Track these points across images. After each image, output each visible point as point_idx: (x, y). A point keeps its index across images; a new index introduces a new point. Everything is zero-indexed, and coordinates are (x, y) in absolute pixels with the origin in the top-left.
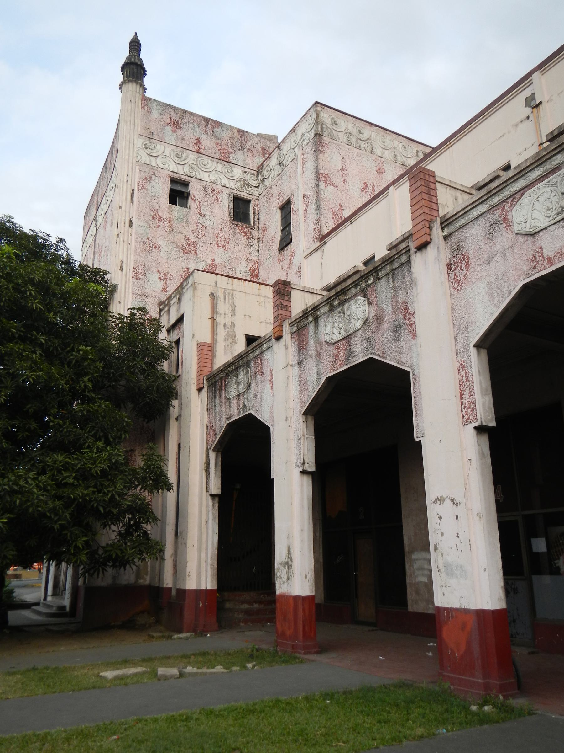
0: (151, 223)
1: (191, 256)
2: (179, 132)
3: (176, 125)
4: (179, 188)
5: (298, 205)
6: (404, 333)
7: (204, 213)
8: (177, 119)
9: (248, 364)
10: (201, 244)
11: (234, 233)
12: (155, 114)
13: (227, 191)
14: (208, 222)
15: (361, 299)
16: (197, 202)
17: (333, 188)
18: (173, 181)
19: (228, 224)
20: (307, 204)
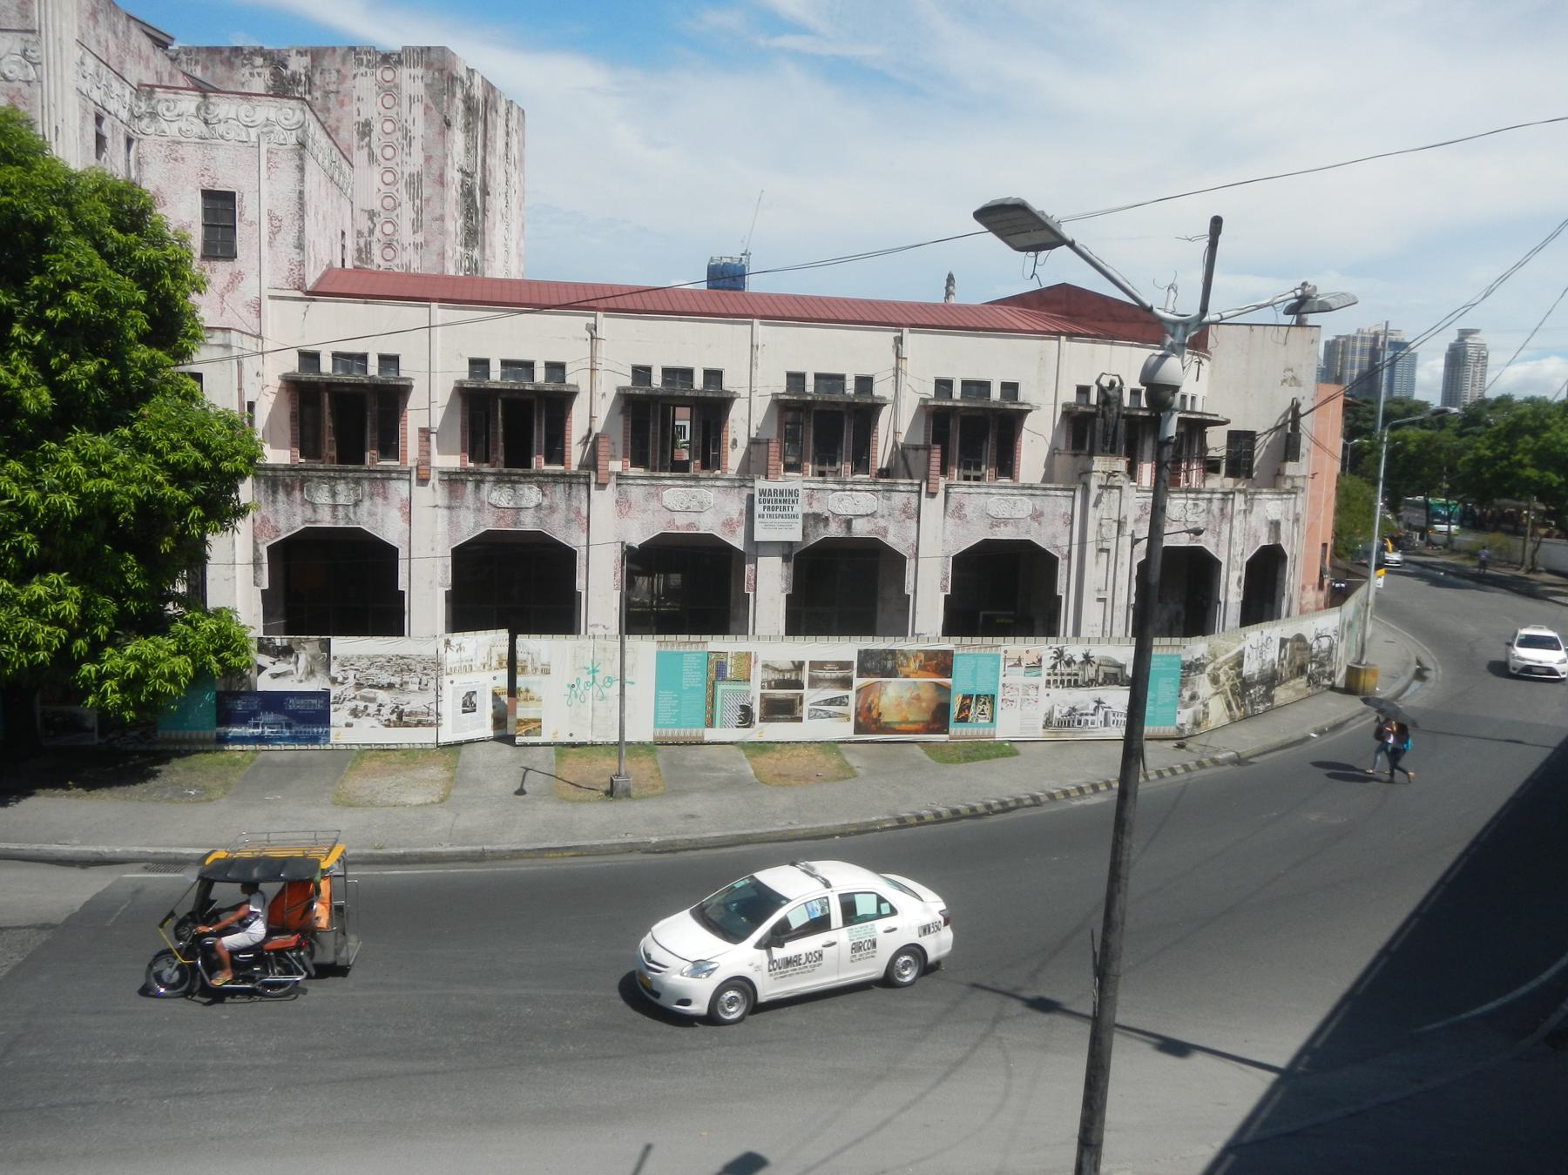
5: (248, 211)
6: (574, 526)
9: (358, 481)
15: (536, 489)
20: (275, 231)
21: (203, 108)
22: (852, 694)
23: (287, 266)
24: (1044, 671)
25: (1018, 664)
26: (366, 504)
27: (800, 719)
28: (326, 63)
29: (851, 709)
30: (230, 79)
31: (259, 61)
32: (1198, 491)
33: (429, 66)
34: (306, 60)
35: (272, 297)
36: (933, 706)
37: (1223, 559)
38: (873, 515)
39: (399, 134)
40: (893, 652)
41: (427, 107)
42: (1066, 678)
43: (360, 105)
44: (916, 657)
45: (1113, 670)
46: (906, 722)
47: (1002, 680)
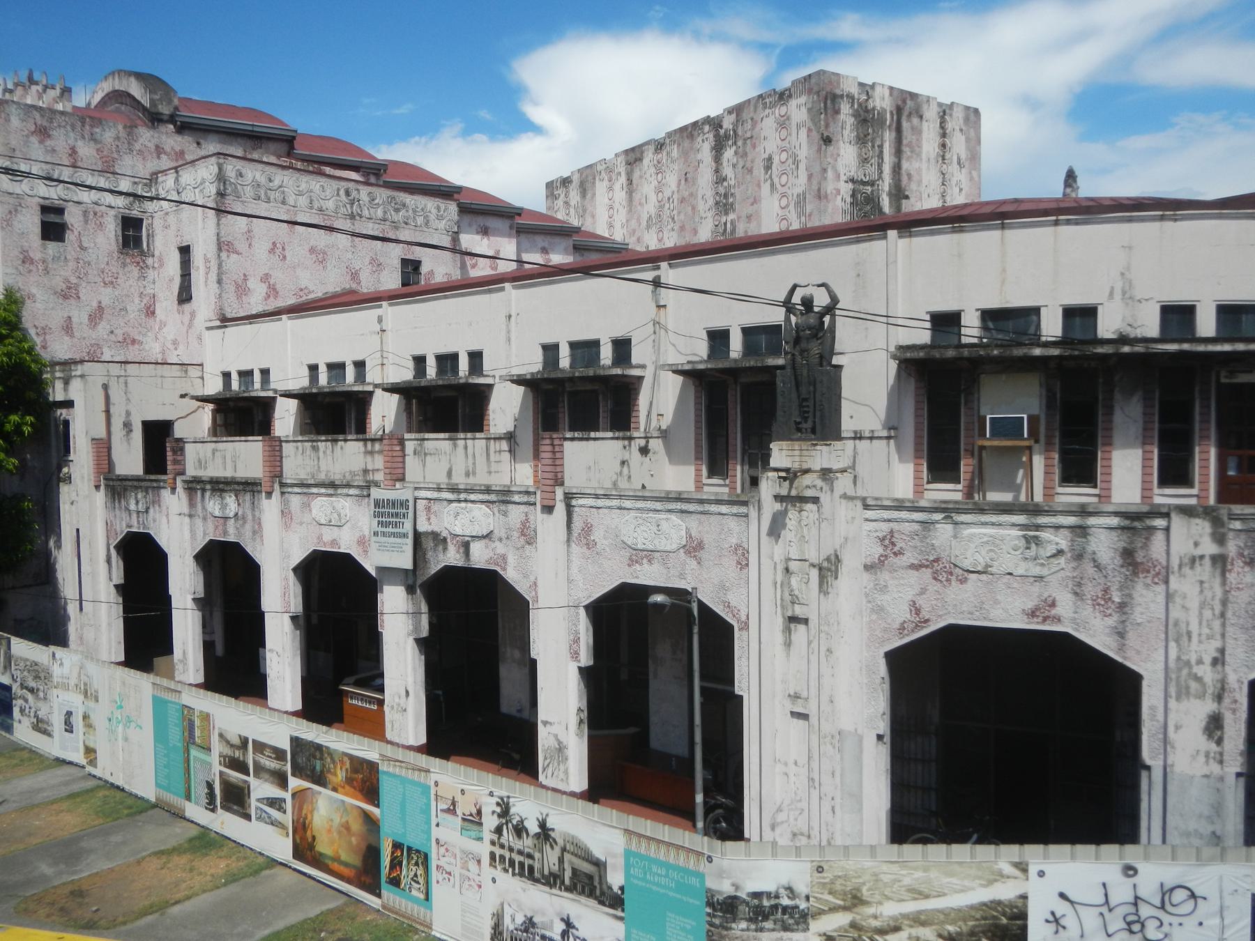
0: (21, 268)
1: (72, 301)
2: (48, 143)
3: (43, 133)
4: (52, 218)
7: (85, 245)
8: (45, 124)
10: (84, 284)
11: (124, 265)
12: (15, 122)
13: (112, 212)
14: (91, 256)
16: (76, 233)
17: (235, 256)
18: (45, 209)
19: (116, 255)
21: (177, 180)
22: (288, 796)
23: (213, 300)
24: (488, 835)
25: (452, 811)
26: (151, 511)
27: (248, 817)
28: (746, 115)
29: (288, 819)
30: (692, 148)
31: (707, 128)
32: (1036, 510)
33: (810, 91)
34: (734, 116)
35: (208, 328)
36: (363, 847)
37: (1148, 664)
38: (488, 536)
39: (790, 161)
40: (319, 747)
41: (810, 130)
42: (518, 858)
43: (765, 143)
44: (342, 762)
45: (586, 867)
46: (336, 859)
47: (435, 833)
